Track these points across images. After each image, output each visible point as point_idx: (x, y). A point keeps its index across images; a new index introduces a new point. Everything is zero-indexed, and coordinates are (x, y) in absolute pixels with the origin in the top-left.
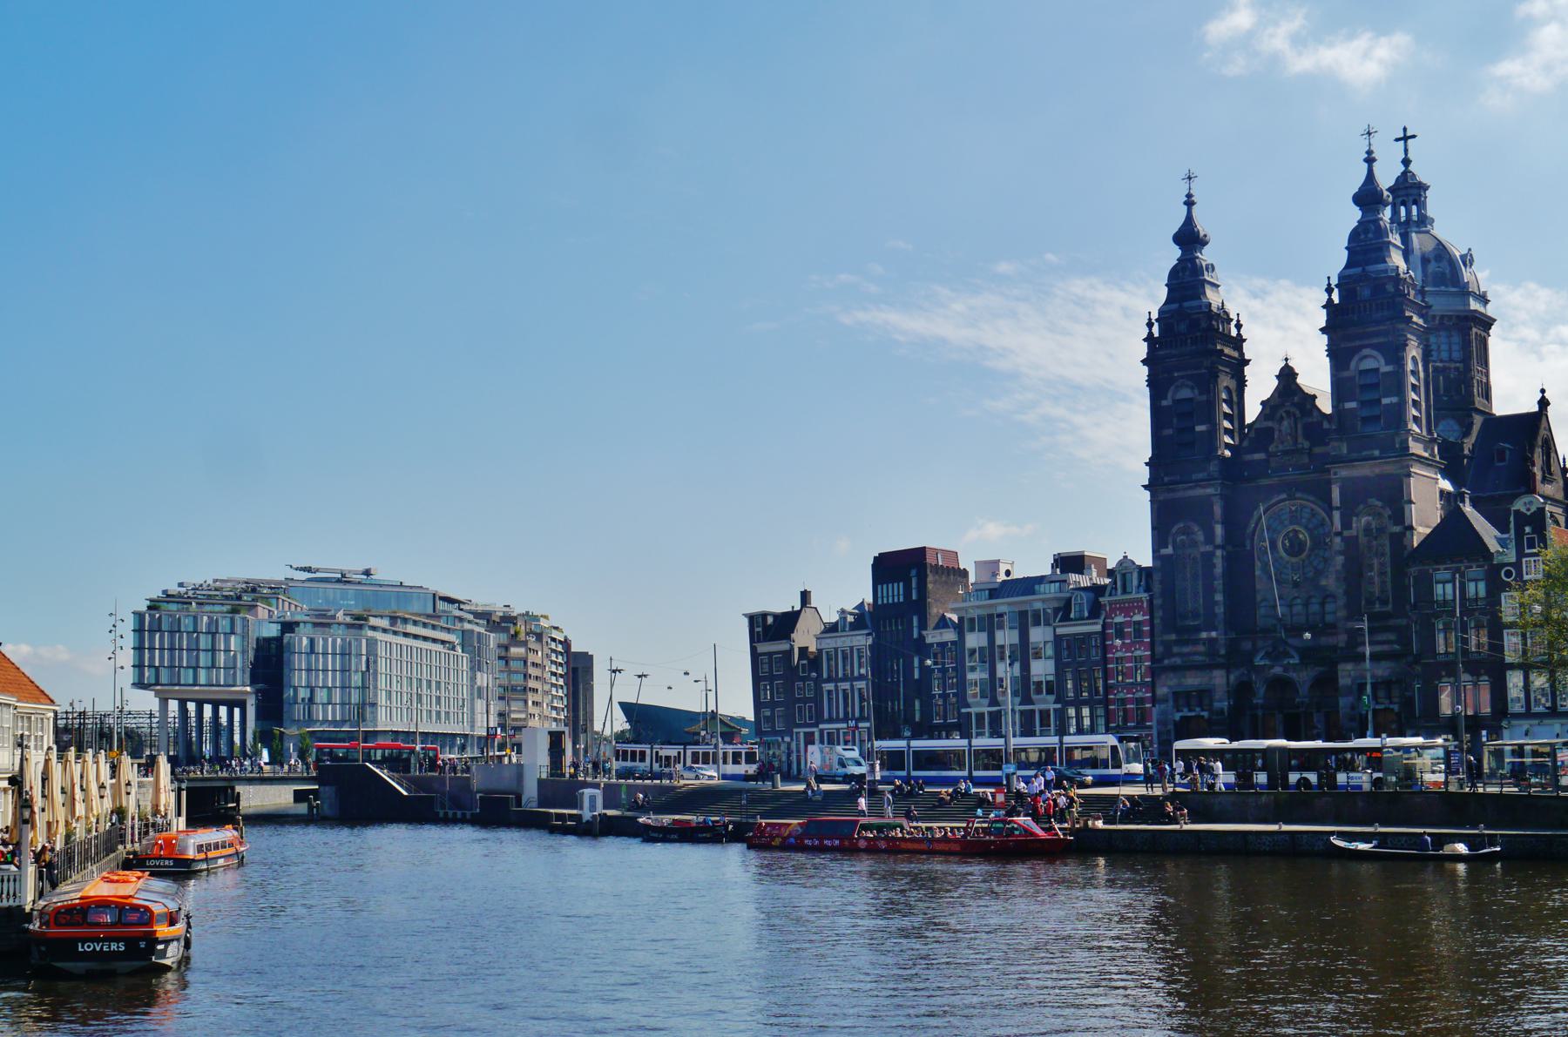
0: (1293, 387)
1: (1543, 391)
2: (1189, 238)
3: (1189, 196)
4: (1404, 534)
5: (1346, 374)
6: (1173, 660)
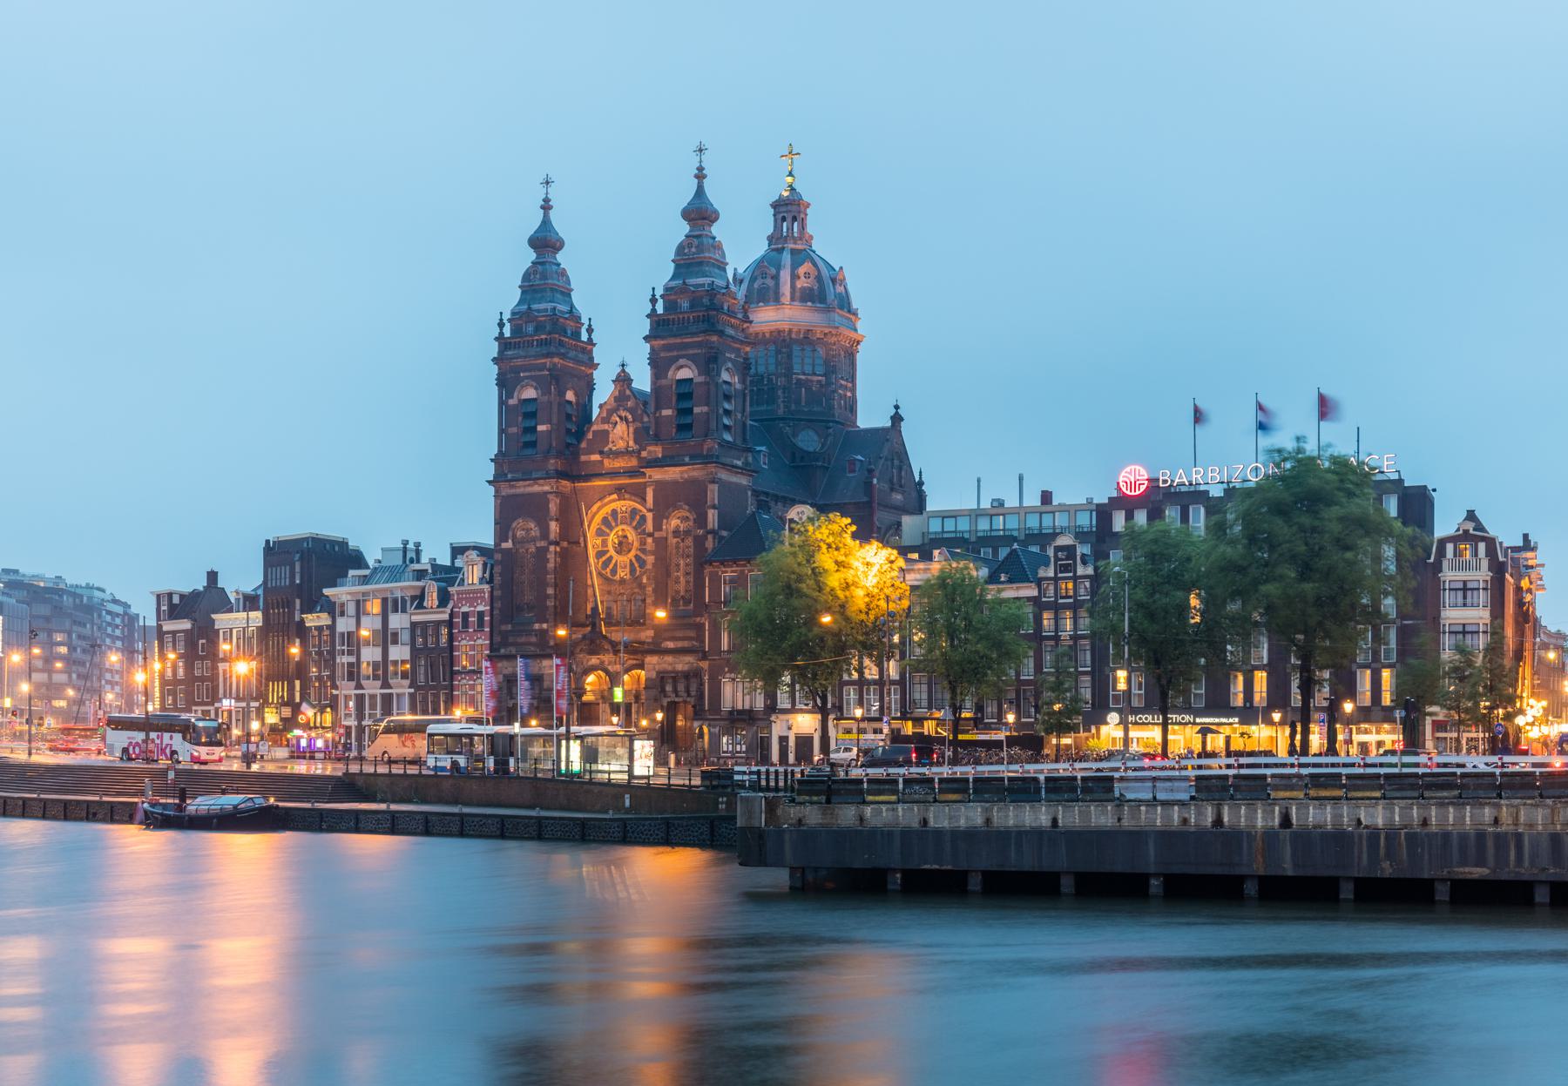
0: (628, 392)
1: (897, 407)
2: (545, 242)
3: (546, 200)
4: (705, 537)
5: (664, 382)
6: (508, 649)
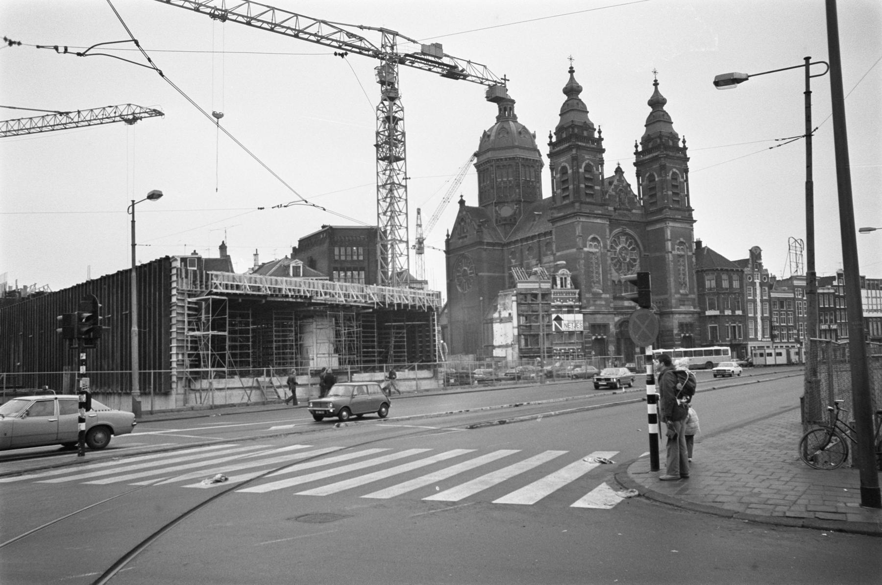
0: (623, 179)
2: (572, 90)
